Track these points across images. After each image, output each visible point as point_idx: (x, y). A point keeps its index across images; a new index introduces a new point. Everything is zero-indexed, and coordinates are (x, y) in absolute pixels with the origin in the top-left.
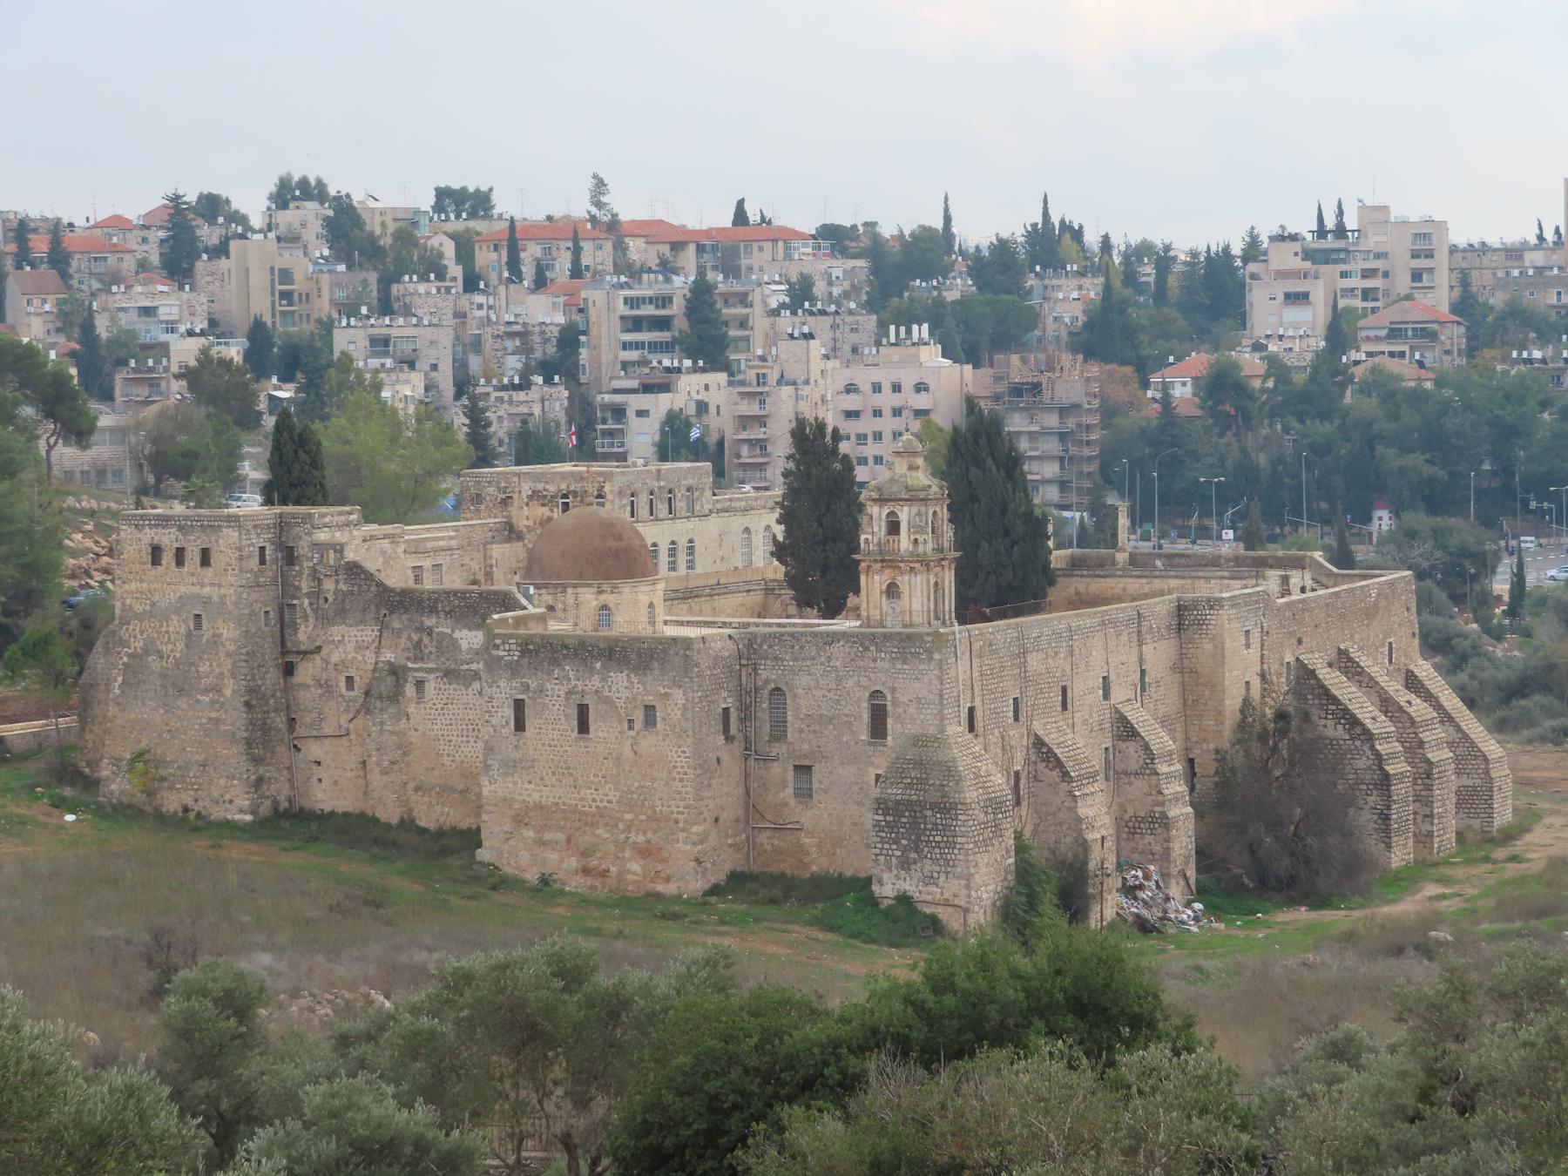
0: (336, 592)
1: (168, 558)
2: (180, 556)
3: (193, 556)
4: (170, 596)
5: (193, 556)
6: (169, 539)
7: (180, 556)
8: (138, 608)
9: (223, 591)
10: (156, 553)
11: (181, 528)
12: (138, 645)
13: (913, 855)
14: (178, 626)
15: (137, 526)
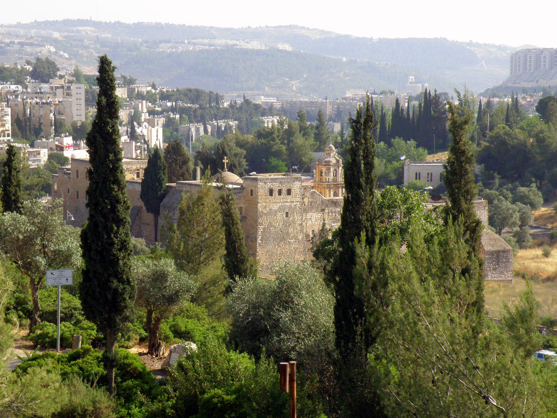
0: (309, 202)
1: (276, 193)
2: (280, 192)
3: (284, 192)
4: (275, 207)
5: (284, 192)
6: (276, 186)
7: (280, 192)
8: (265, 212)
9: (295, 204)
10: (271, 192)
11: (280, 183)
12: (266, 224)
13: (497, 266)
14: (280, 216)
15: (265, 183)
